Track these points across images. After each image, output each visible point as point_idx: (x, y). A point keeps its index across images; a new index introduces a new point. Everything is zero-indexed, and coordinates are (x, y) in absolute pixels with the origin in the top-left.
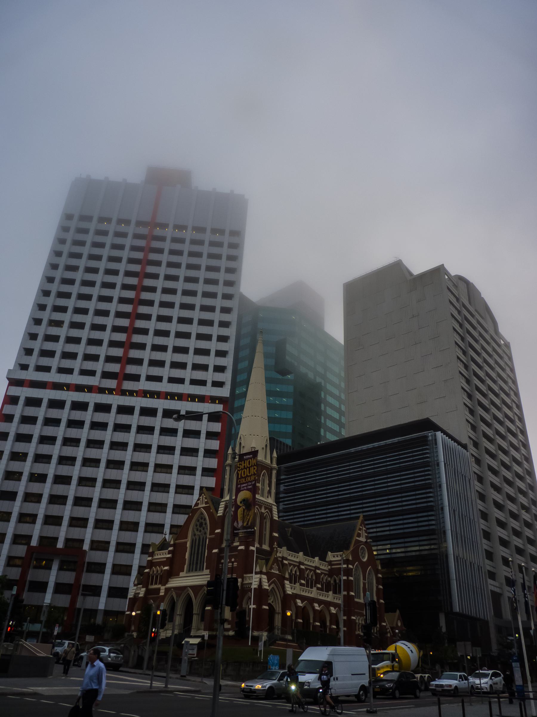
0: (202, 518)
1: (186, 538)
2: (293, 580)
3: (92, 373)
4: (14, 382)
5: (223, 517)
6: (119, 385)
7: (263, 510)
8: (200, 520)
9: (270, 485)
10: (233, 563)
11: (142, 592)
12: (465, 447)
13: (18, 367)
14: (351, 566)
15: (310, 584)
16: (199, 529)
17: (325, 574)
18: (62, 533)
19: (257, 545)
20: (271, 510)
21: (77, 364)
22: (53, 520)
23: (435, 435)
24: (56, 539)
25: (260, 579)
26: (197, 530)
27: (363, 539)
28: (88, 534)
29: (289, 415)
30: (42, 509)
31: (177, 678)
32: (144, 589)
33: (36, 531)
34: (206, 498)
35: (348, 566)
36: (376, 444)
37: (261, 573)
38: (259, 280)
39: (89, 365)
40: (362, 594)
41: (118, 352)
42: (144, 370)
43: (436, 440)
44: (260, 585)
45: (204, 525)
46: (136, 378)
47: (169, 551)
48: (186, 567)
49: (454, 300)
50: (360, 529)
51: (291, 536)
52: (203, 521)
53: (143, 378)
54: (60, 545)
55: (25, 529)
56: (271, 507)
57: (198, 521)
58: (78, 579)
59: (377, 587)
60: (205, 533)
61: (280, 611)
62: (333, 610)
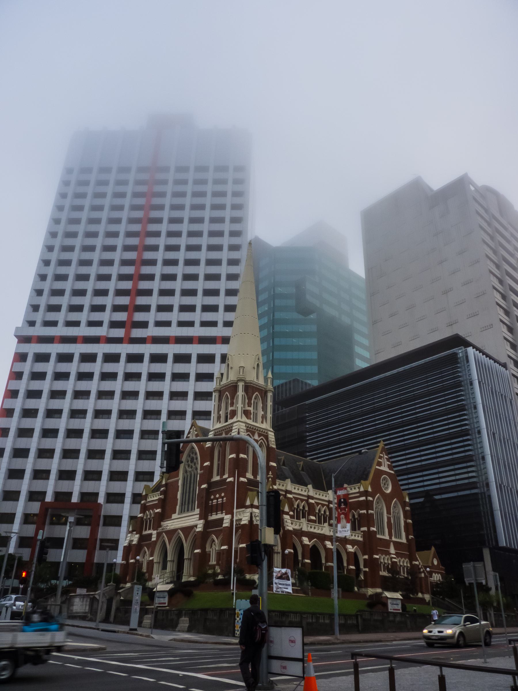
0: (193, 453)
1: (178, 476)
2: (298, 515)
3: (99, 324)
4: (24, 340)
6: (128, 333)
8: (191, 455)
9: (264, 408)
10: (223, 498)
11: (135, 538)
12: (504, 365)
13: (27, 325)
14: (370, 498)
15: (322, 519)
16: (191, 464)
18: (76, 488)
19: (249, 475)
20: (267, 437)
21: (83, 317)
22: (67, 475)
23: (466, 352)
24: (70, 494)
25: (251, 514)
26: (189, 466)
27: (384, 468)
28: (103, 487)
29: (314, 355)
30: (54, 465)
31: (124, 632)
32: (137, 536)
33: (50, 487)
34: (196, 431)
35: (366, 498)
36: (401, 369)
37: (252, 506)
38: (274, 219)
39: (96, 316)
40: (386, 530)
41: (125, 300)
42: (151, 317)
43: (467, 357)
44: (251, 521)
45: (195, 460)
46: (144, 325)
47: (161, 492)
48: (178, 507)
49: (482, 211)
50: (380, 457)
51: (303, 470)
52: (194, 457)
53: (151, 324)
54: (75, 499)
55: (39, 485)
56: (267, 433)
57: (190, 456)
58: (94, 532)
59: (405, 522)
60: (196, 469)
61: (280, 550)
62: (350, 548)
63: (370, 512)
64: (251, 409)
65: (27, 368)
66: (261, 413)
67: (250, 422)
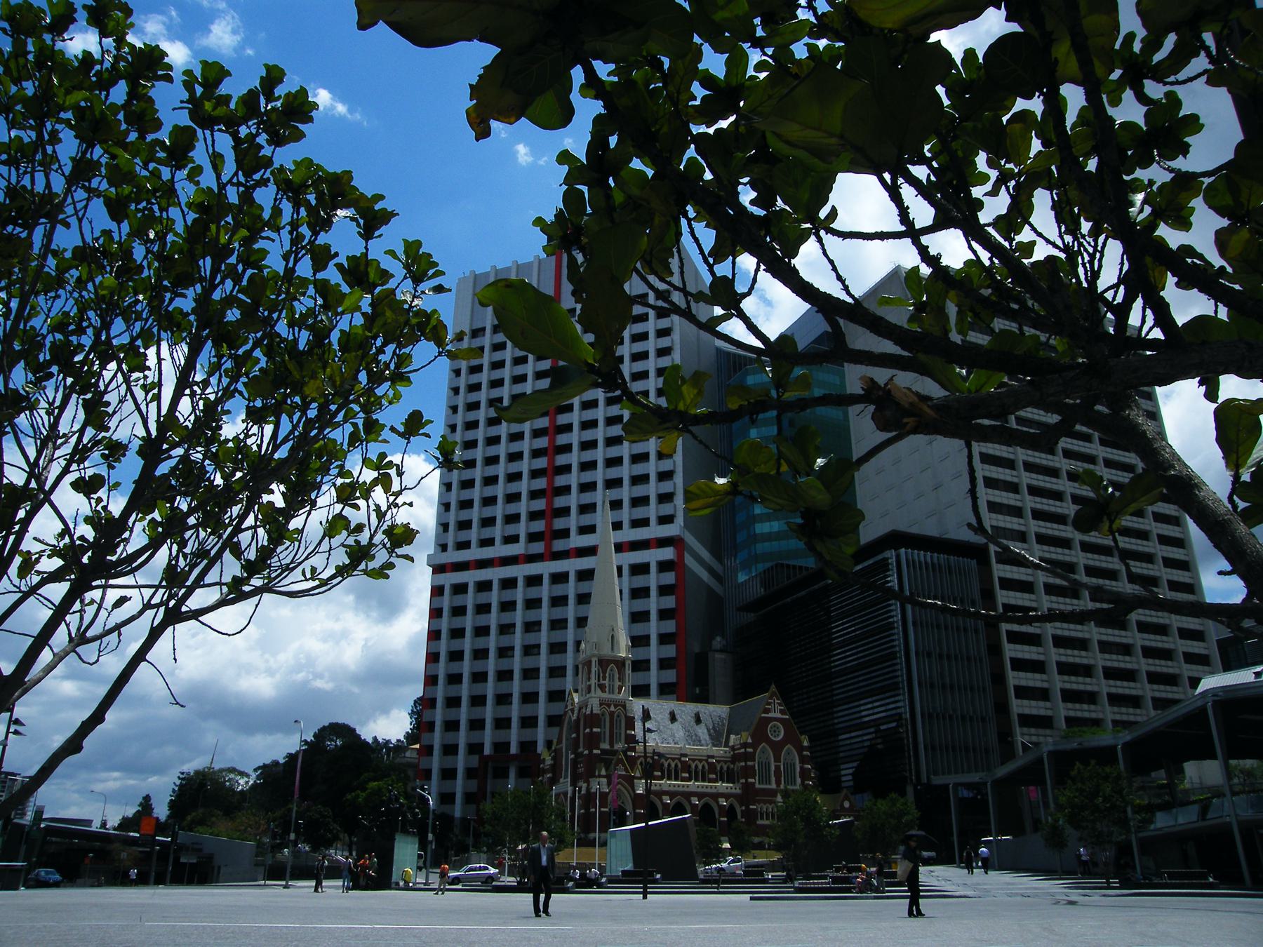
4: (438, 569)
7: (612, 709)
17: (726, 762)
18: (514, 736)
20: (624, 706)
21: (497, 531)
23: (898, 556)
24: (507, 745)
33: (488, 737)
37: (600, 776)
42: (573, 522)
46: (565, 533)
50: (769, 704)
54: (514, 749)
55: (475, 737)
59: (802, 768)
63: (750, 763)
64: (606, 682)
65: (446, 602)
66: (617, 683)
67: (605, 696)
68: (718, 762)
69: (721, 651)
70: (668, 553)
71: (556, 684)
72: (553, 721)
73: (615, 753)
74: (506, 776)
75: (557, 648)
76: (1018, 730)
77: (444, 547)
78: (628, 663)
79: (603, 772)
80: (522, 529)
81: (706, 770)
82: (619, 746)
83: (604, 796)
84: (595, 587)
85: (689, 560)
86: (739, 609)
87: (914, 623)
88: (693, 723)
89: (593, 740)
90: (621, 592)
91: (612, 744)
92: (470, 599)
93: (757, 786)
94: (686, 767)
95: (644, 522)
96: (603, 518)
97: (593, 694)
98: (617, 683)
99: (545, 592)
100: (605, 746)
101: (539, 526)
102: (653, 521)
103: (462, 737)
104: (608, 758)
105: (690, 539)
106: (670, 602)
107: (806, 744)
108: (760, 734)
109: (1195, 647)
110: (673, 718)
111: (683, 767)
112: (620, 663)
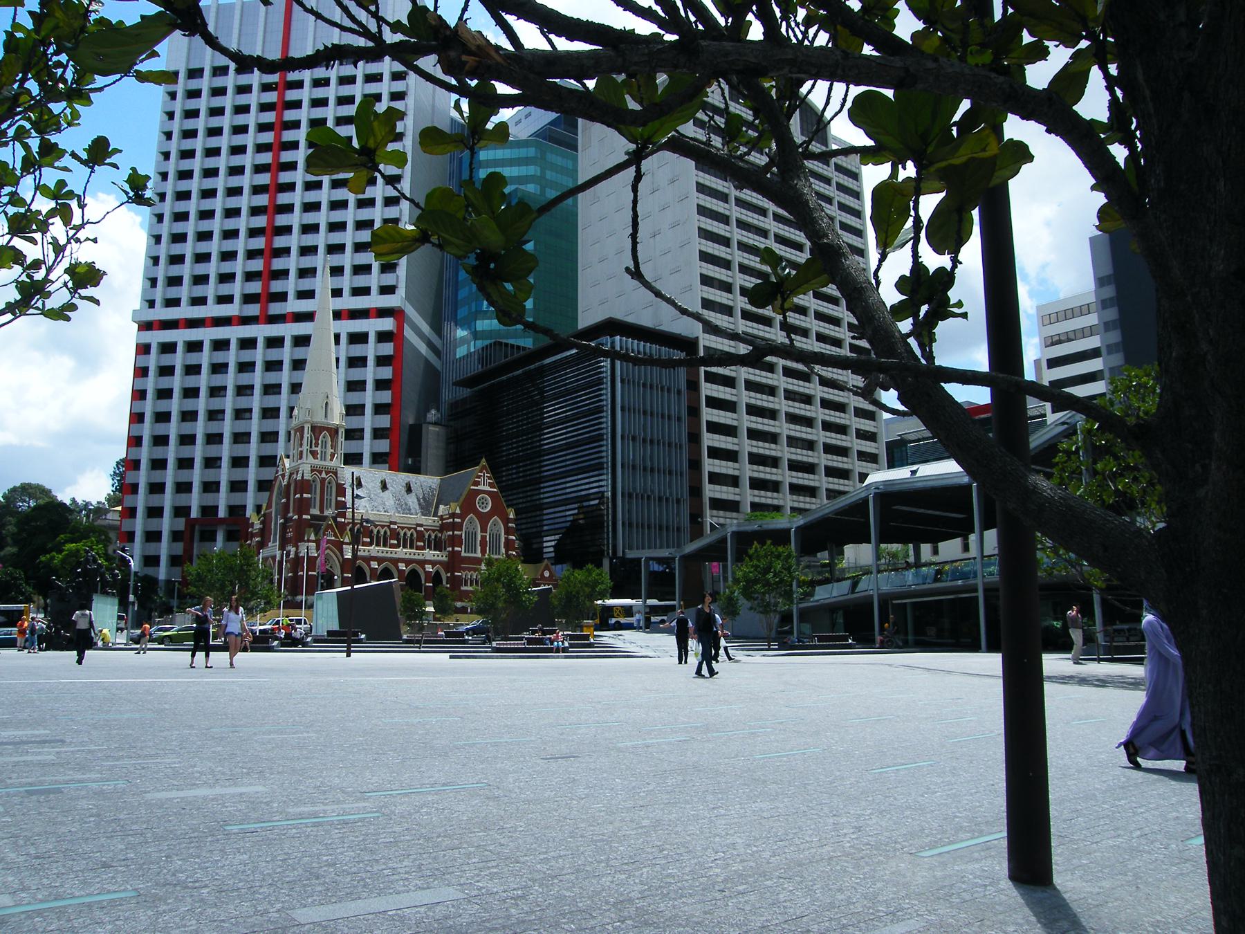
4: (145, 326)
5: (289, 485)
6: (264, 309)
17: (434, 531)
18: (222, 500)
20: (336, 474)
21: (210, 290)
33: (195, 501)
37: (309, 541)
40: (479, 548)
42: (291, 285)
46: (282, 297)
53: (291, 296)
54: (222, 513)
55: (182, 500)
64: (319, 449)
65: (152, 361)
66: (330, 450)
67: (318, 462)
68: (427, 530)
69: (435, 424)
70: (387, 324)
71: (268, 449)
72: (263, 486)
73: (324, 518)
74: (213, 539)
75: (270, 413)
76: (708, 512)
77: (151, 304)
78: (341, 431)
79: (313, 537)
80: (237, 288)
81: (417, 538)
82: (329, 512)
83: (312, 560)
84: (309, 353)
85: (408, 333)
86: (455, 384)
87: (623, 409)
88: (403, 492)
89: (303, 506)
90: (337, 360)
91: (322, 511)
92: (178, 360)
93: (463, 554)
94: (395, 534)
95: (365, 291)
96: (322, 283)
97: (304, 460)
98: (330, 450)
99: (259, 355)
100: (315, 511)
101: (255, 287)
102: (374, 290)
103: (168, 500)
104: (317, 524)
105: (410, 311)
106: (387, 373)
107: (511, 516)
108: (469, 506)
109: (868, 447)
110: (384, 487)
111: (392, 535)
112: (334, 431)
